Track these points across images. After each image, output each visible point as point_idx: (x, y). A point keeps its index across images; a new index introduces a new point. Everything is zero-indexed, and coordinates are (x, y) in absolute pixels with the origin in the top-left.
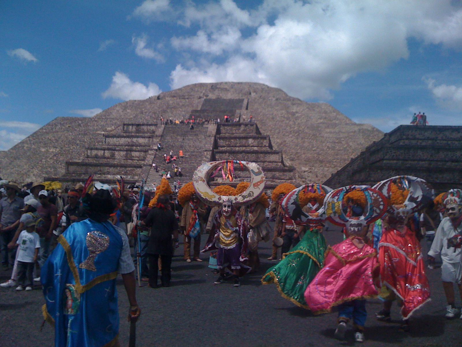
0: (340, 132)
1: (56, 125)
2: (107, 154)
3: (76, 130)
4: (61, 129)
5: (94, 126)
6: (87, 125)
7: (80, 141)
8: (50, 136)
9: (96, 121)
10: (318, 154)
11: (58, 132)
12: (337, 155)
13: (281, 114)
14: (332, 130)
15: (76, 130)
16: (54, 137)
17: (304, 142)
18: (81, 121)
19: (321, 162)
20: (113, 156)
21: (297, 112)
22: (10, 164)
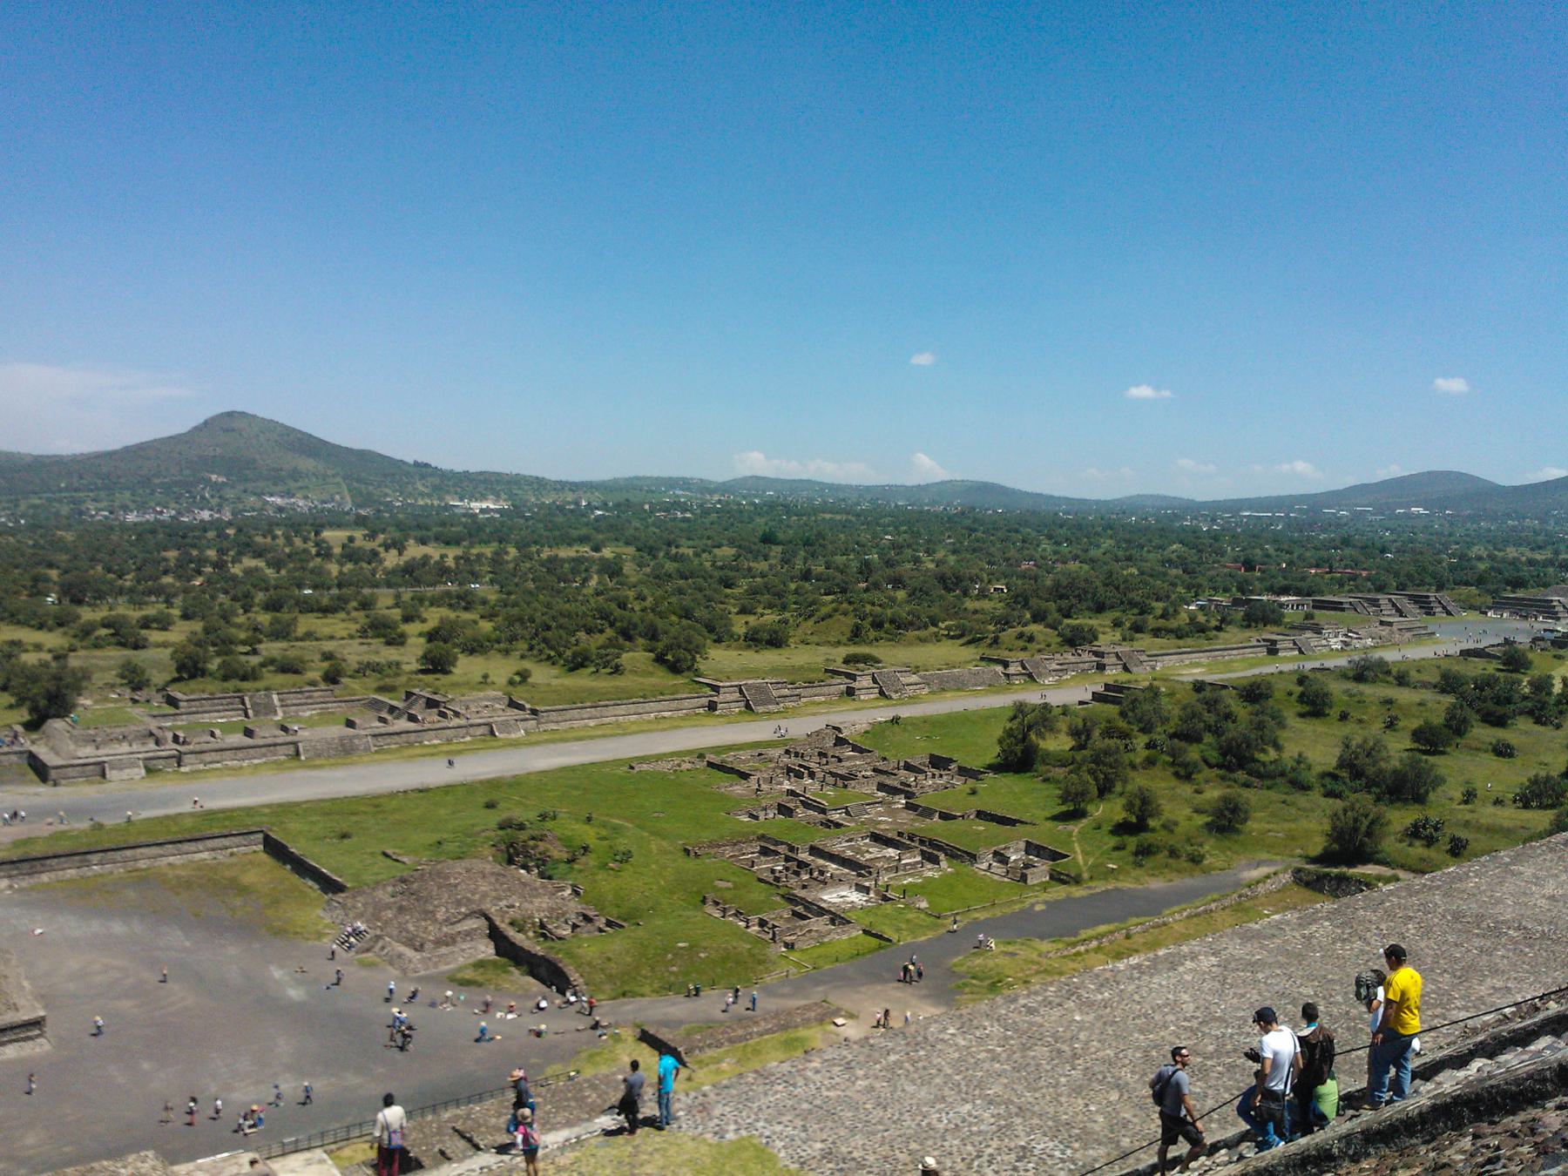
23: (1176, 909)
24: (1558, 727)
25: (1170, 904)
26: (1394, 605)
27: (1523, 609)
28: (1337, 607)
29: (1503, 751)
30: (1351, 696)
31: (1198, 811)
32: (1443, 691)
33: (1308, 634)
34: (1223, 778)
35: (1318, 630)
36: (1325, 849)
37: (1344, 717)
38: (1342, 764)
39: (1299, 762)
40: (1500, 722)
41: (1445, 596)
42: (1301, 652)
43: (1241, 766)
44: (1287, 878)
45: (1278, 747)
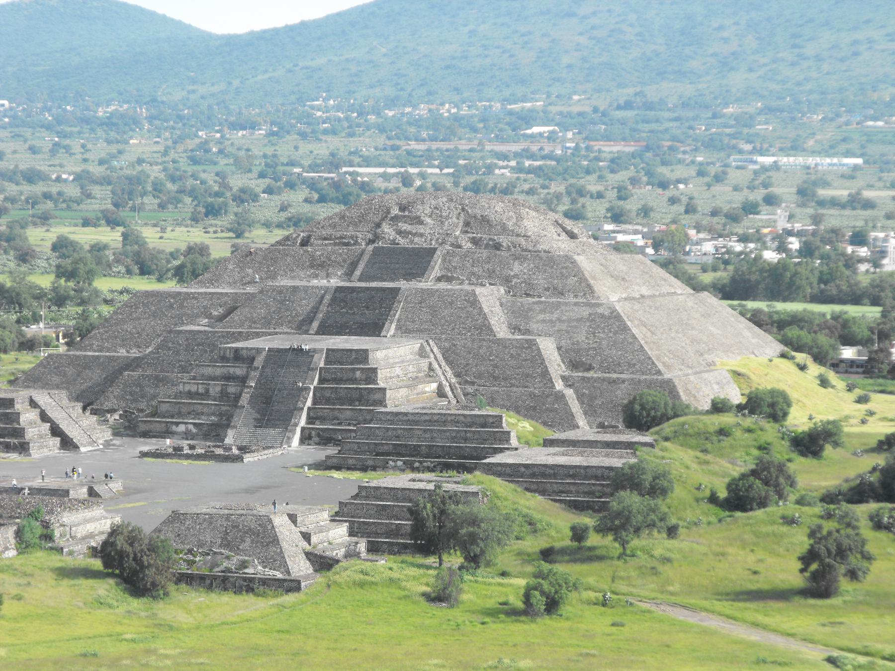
0: (559, 320)
1: (137, 308)
2: (201, 390)
3: (166, 316)
4: (145, 313)
5: (192, 308)
6: (182, 306)
7: (173, 343)
8: (128, 327)
9: (196, 299)
10: (496, 366)
11: (140, 319)
12: (519, 368)
13: (465, 296)
14: (547, 316)
15: (166, 316)
16: (135, 328)
17: (480, 347)
18: (174, 298)
19: (496, 378)
20: (207, 391)
21: (516, 276)
22: (78, 376)
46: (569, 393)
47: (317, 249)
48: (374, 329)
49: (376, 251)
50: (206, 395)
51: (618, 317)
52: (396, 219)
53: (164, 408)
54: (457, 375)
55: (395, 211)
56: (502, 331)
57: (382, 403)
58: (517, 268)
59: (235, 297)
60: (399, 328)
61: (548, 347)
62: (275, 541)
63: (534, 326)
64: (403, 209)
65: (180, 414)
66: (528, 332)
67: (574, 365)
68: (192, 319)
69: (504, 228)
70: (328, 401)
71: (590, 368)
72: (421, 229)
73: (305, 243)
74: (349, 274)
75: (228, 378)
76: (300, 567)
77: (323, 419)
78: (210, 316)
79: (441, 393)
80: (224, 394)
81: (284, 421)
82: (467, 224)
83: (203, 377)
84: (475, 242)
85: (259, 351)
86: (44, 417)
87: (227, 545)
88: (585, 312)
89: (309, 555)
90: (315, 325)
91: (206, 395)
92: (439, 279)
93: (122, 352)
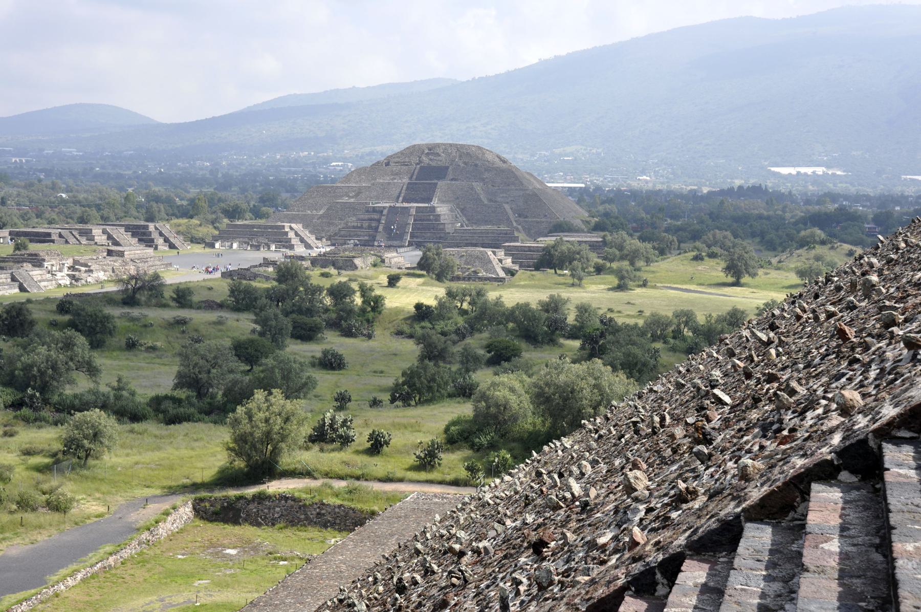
23: (63, 572)
24: (370, 337)
25: (53, 570)
26: (110, 237)
27: (252, 238)
28: (44, 238)
29: (331, 363)
30: (133, 319)
31: (28, 453)
32: (237, 309)
33: (28, 266)
34: (27, 420)
35: (37, 261)
36: (222, 471)
37: (131, 346)
38: (183, 381)
39: (120, 389)
40: (306, 334)
41: (167, 228)
42: (22, 289)
43: (46, 402)
44: (186, 511)
45: (92, 371)
46: (520, 227)
47: (394, 167)
48: (429, 200)
49: (421, 168)
50: (361, 227)
51: (536, 195)
52: (428, 154)
53: (342, 233)
54: (468, 220)
55: (427, 151)
56: (486, 202)
57: (443, 229)
58: (486, 175)
59: (360, 188)
60: (439, 200)
61: (507, 207)
62: (490, 262)
63: (499, 199)
64: (430, 150)
65: (350, 236)
66: (496, 201)
67: (520, 216)
68: (341, 197)
69: (478, 158)
70: (419, 229)
71: (526, 217)
72: (440, 158)
73: (387, 164)
74: (411, 178)
75: (371, 220)
76: (502, 274)
77: (417, 237)
78: (349, 196)
79: (462, 226)
80: (370, 227)
81: (400, 237)
82: (460, 156)
83: (359, 219)
84: (465, 163)
85: (384, 208)
86: (297, 234)
87: (468, 264)
88: (521, 193)
89: (504, 269)
90: (401, 199)
91: (361, 227)
92: (452, 180)
93: (309, 212)
